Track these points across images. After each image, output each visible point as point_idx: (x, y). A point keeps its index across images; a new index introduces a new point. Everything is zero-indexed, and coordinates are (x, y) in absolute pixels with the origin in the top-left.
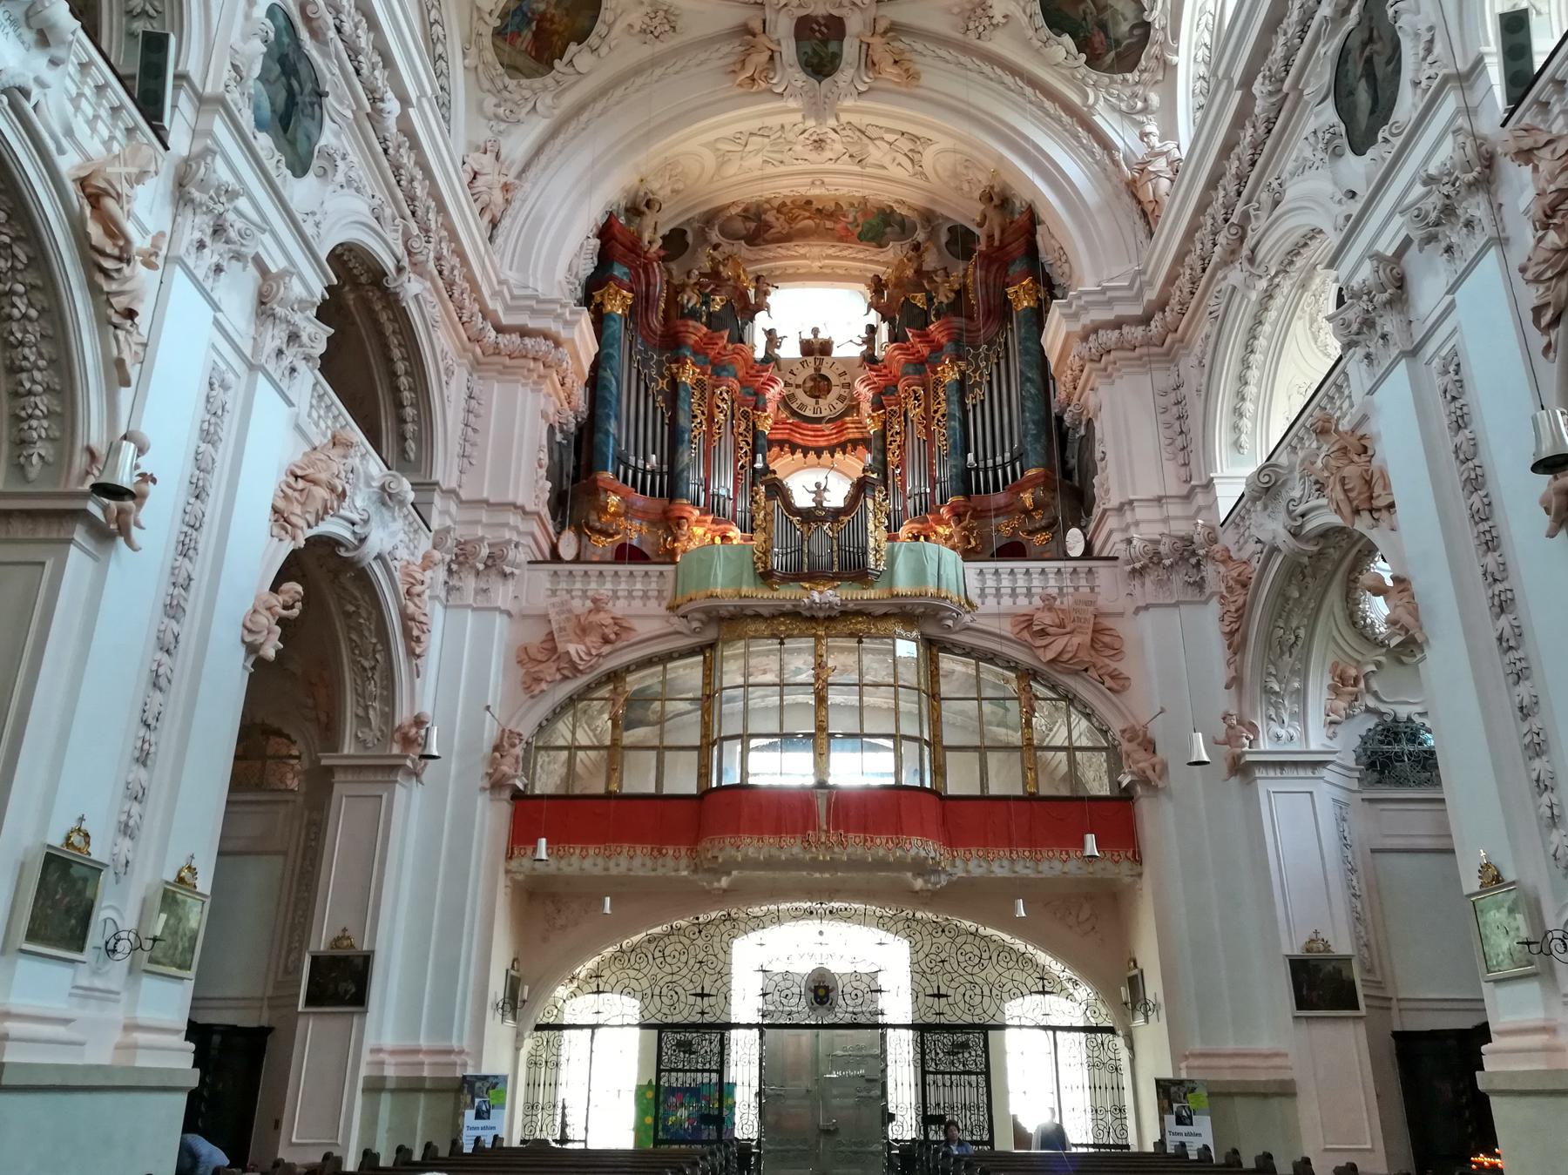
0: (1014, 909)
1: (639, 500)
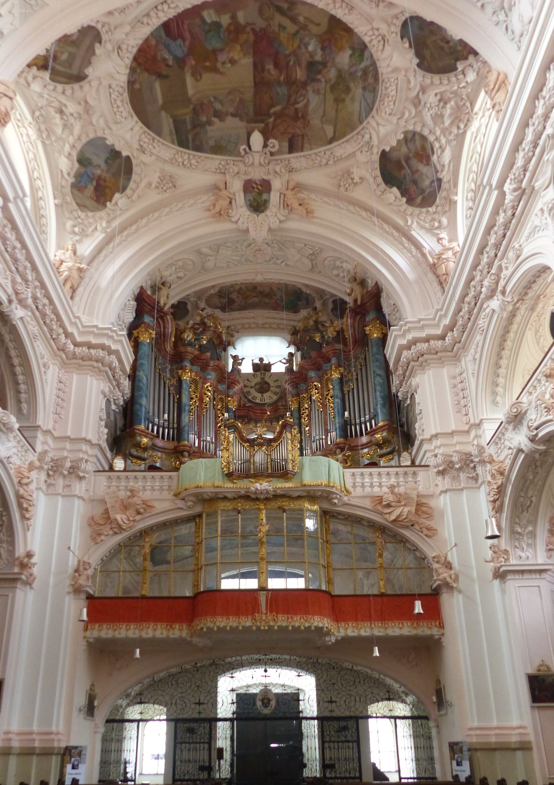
0: (372, 651)
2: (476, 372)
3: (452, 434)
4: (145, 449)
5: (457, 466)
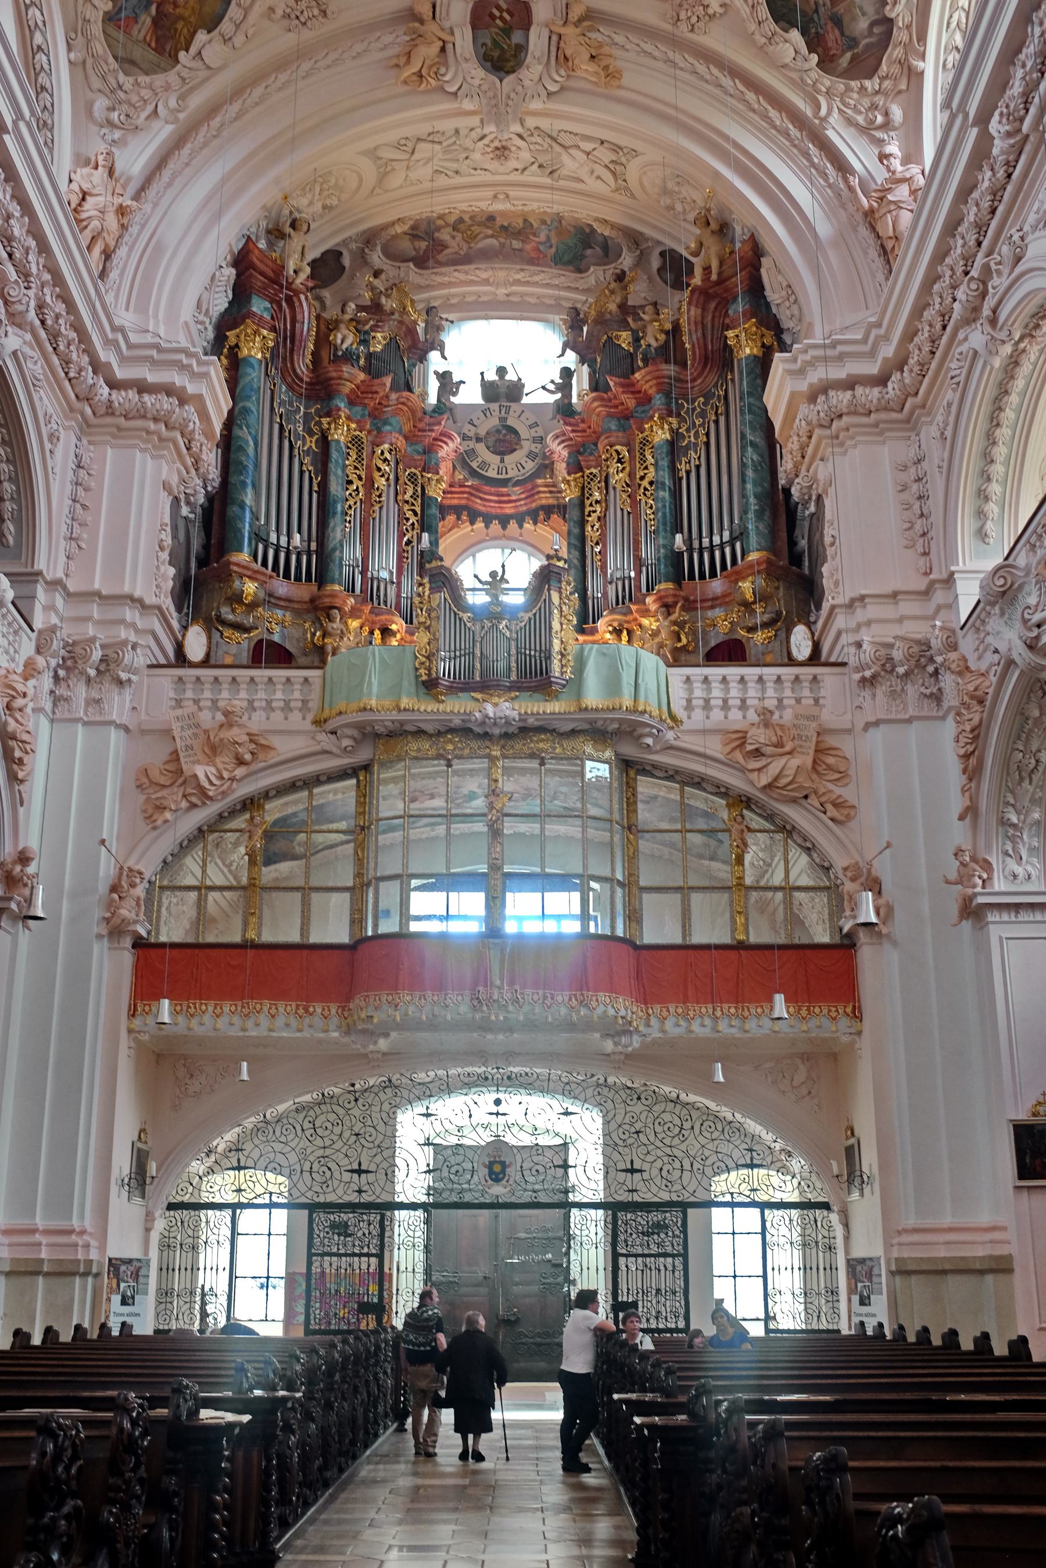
1: (282, 587)
2: (945, 465)
3: (895, 595)
4: (253, 606)
5: (901, 670)
